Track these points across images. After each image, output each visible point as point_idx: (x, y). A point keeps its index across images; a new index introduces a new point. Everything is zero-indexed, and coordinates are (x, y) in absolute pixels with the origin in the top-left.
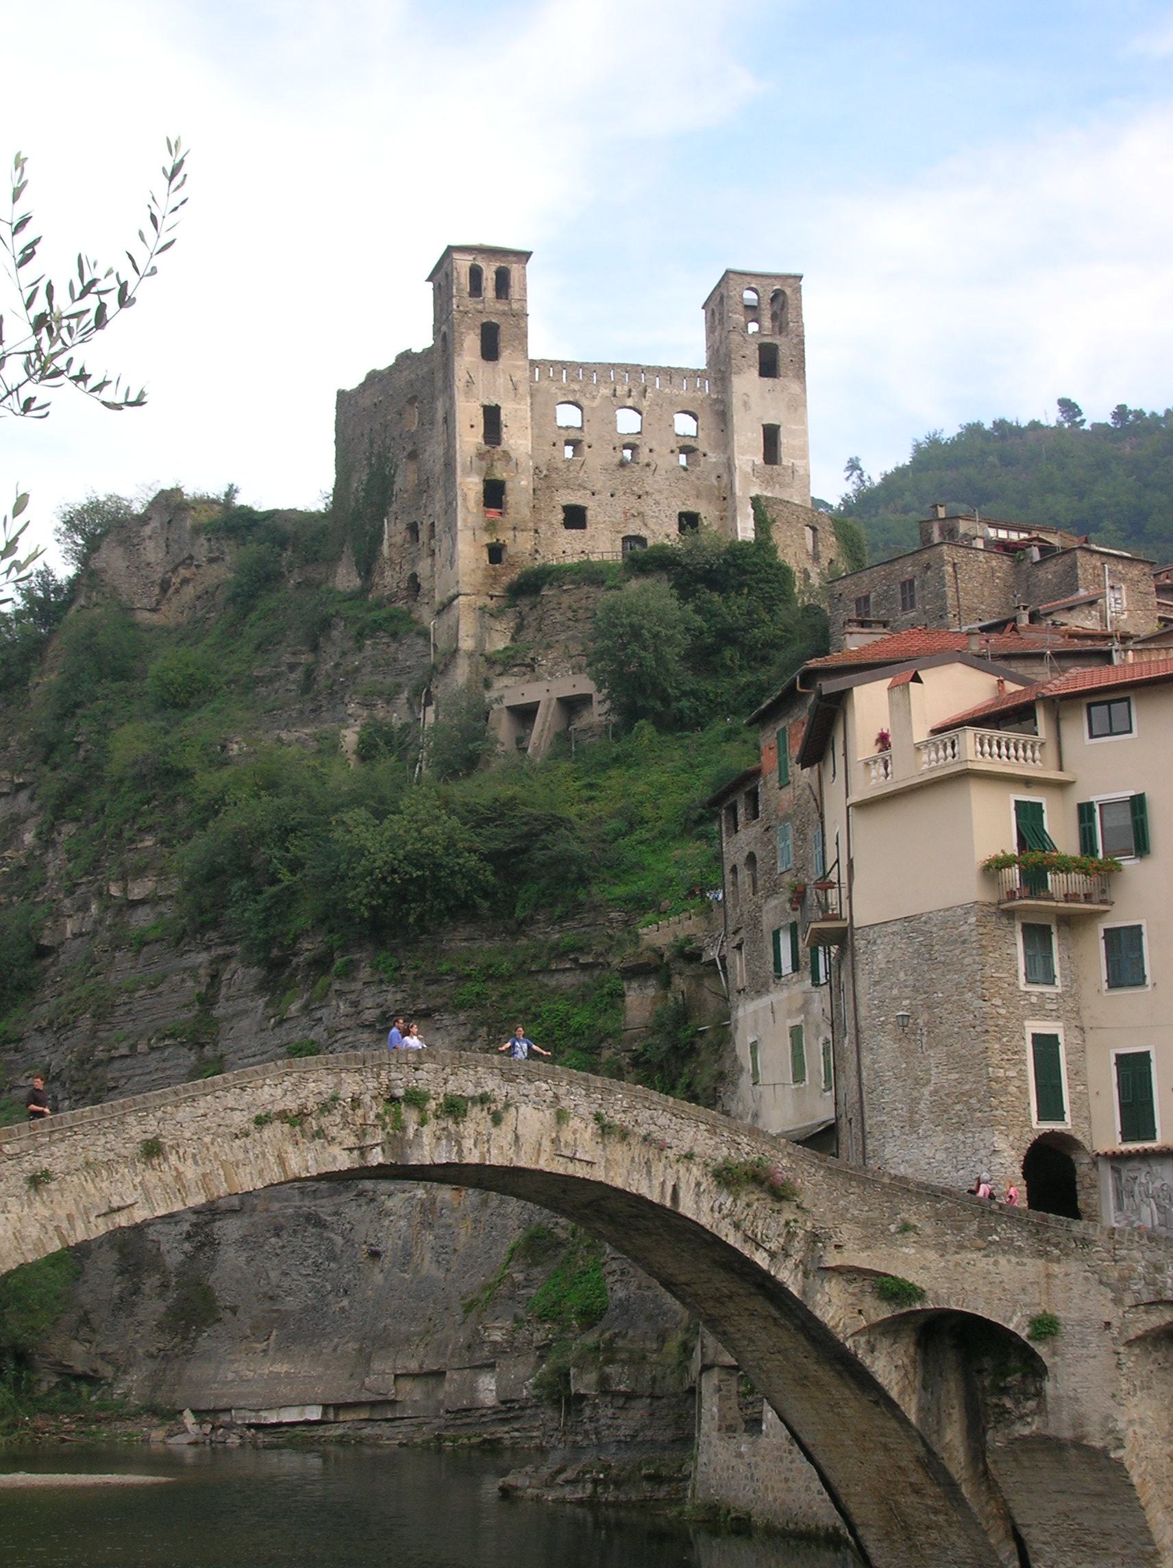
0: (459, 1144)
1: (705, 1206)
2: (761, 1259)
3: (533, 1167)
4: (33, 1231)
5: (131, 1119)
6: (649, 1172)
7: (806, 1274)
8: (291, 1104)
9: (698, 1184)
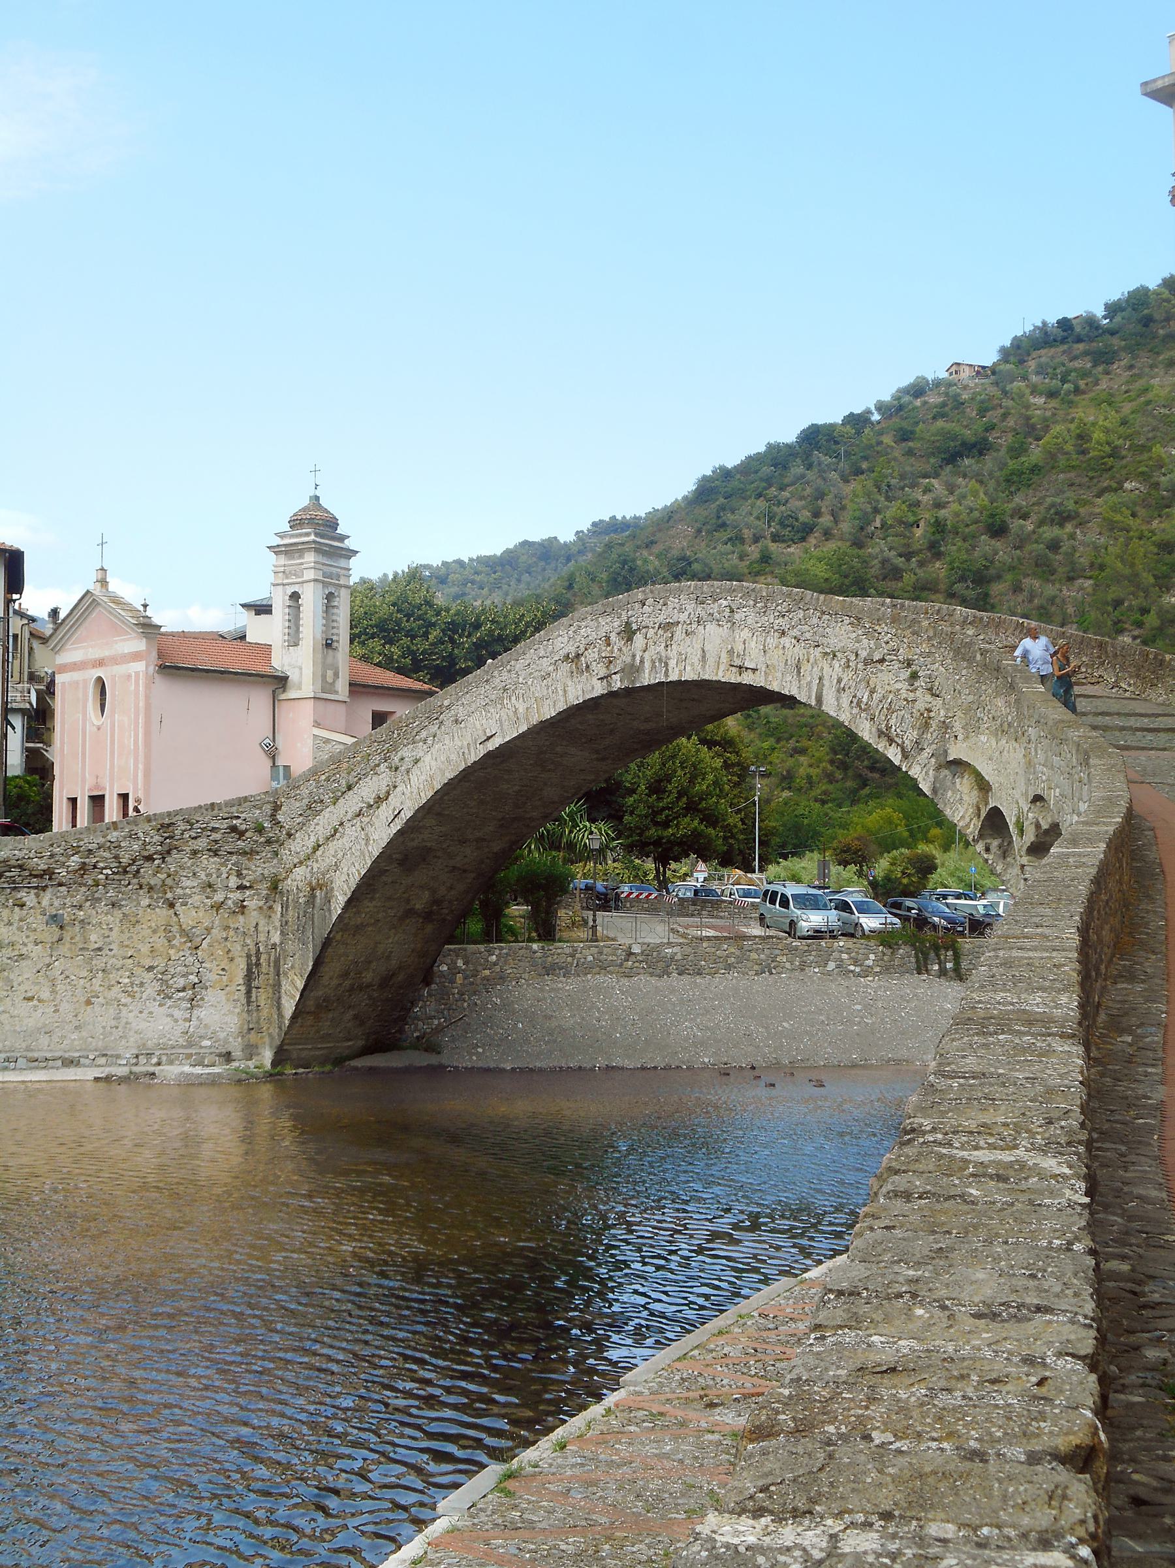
0: (666, 664)
1: (845, 700)
2: (894, 755)
3: (714, 678)
4: (453, 757)
5: (496, 673)
6: (799, 672)
7: (938, 768)
8: (572, 650)
9: (839, 681)
